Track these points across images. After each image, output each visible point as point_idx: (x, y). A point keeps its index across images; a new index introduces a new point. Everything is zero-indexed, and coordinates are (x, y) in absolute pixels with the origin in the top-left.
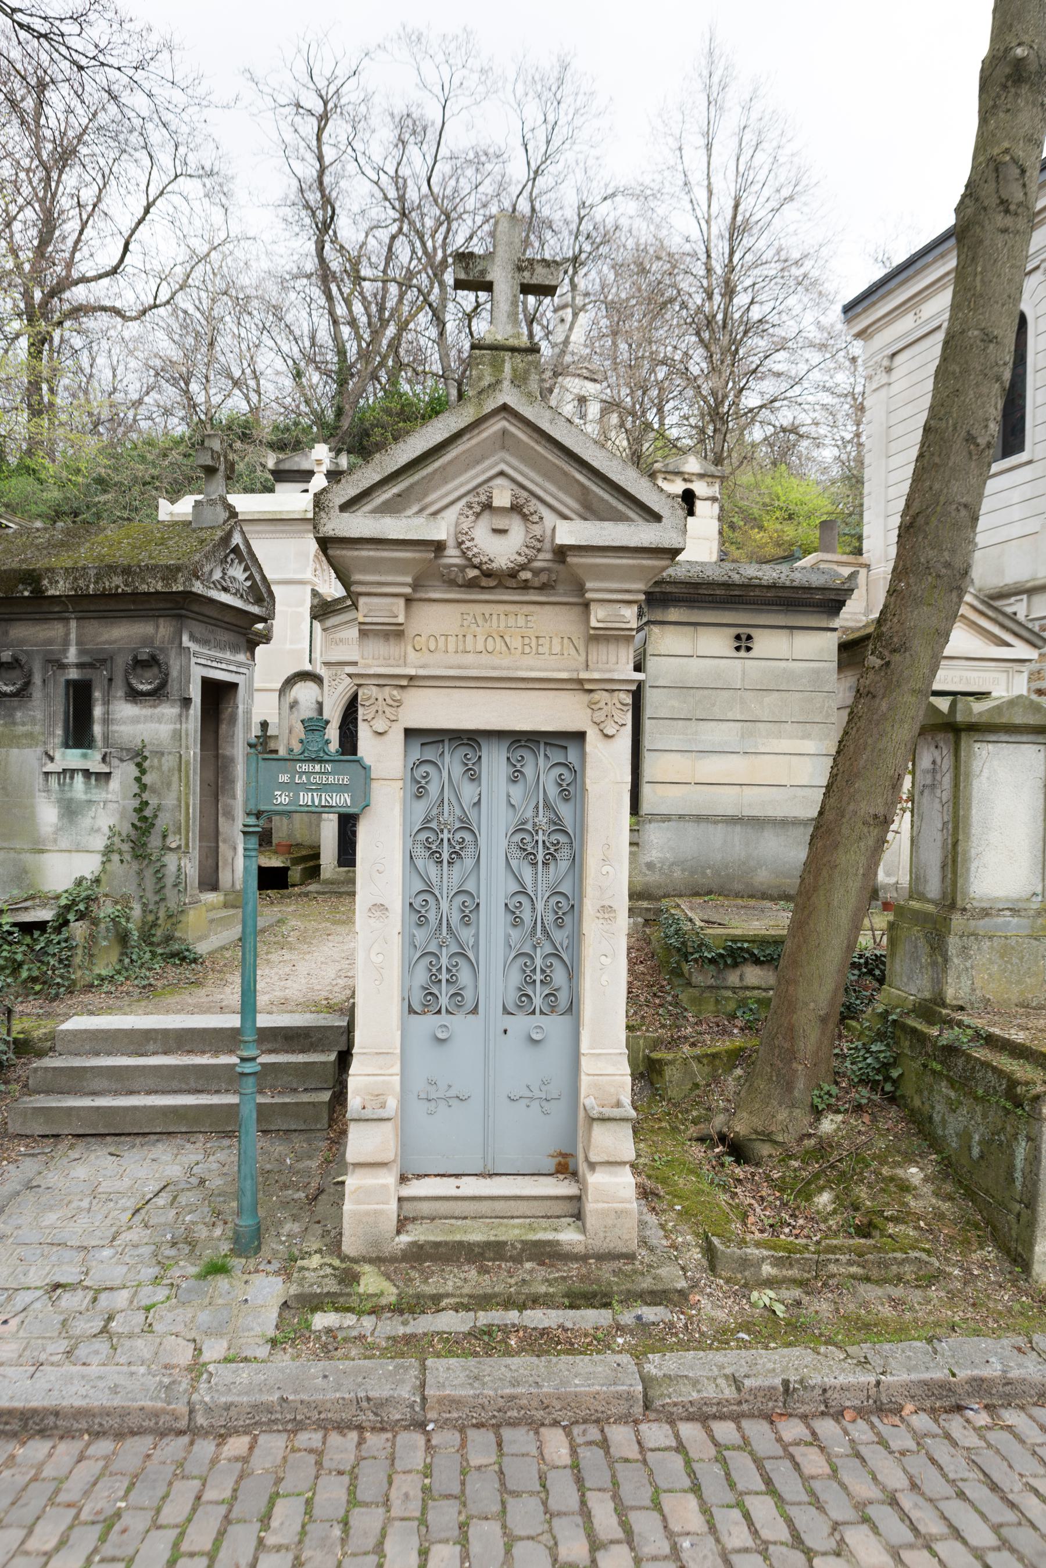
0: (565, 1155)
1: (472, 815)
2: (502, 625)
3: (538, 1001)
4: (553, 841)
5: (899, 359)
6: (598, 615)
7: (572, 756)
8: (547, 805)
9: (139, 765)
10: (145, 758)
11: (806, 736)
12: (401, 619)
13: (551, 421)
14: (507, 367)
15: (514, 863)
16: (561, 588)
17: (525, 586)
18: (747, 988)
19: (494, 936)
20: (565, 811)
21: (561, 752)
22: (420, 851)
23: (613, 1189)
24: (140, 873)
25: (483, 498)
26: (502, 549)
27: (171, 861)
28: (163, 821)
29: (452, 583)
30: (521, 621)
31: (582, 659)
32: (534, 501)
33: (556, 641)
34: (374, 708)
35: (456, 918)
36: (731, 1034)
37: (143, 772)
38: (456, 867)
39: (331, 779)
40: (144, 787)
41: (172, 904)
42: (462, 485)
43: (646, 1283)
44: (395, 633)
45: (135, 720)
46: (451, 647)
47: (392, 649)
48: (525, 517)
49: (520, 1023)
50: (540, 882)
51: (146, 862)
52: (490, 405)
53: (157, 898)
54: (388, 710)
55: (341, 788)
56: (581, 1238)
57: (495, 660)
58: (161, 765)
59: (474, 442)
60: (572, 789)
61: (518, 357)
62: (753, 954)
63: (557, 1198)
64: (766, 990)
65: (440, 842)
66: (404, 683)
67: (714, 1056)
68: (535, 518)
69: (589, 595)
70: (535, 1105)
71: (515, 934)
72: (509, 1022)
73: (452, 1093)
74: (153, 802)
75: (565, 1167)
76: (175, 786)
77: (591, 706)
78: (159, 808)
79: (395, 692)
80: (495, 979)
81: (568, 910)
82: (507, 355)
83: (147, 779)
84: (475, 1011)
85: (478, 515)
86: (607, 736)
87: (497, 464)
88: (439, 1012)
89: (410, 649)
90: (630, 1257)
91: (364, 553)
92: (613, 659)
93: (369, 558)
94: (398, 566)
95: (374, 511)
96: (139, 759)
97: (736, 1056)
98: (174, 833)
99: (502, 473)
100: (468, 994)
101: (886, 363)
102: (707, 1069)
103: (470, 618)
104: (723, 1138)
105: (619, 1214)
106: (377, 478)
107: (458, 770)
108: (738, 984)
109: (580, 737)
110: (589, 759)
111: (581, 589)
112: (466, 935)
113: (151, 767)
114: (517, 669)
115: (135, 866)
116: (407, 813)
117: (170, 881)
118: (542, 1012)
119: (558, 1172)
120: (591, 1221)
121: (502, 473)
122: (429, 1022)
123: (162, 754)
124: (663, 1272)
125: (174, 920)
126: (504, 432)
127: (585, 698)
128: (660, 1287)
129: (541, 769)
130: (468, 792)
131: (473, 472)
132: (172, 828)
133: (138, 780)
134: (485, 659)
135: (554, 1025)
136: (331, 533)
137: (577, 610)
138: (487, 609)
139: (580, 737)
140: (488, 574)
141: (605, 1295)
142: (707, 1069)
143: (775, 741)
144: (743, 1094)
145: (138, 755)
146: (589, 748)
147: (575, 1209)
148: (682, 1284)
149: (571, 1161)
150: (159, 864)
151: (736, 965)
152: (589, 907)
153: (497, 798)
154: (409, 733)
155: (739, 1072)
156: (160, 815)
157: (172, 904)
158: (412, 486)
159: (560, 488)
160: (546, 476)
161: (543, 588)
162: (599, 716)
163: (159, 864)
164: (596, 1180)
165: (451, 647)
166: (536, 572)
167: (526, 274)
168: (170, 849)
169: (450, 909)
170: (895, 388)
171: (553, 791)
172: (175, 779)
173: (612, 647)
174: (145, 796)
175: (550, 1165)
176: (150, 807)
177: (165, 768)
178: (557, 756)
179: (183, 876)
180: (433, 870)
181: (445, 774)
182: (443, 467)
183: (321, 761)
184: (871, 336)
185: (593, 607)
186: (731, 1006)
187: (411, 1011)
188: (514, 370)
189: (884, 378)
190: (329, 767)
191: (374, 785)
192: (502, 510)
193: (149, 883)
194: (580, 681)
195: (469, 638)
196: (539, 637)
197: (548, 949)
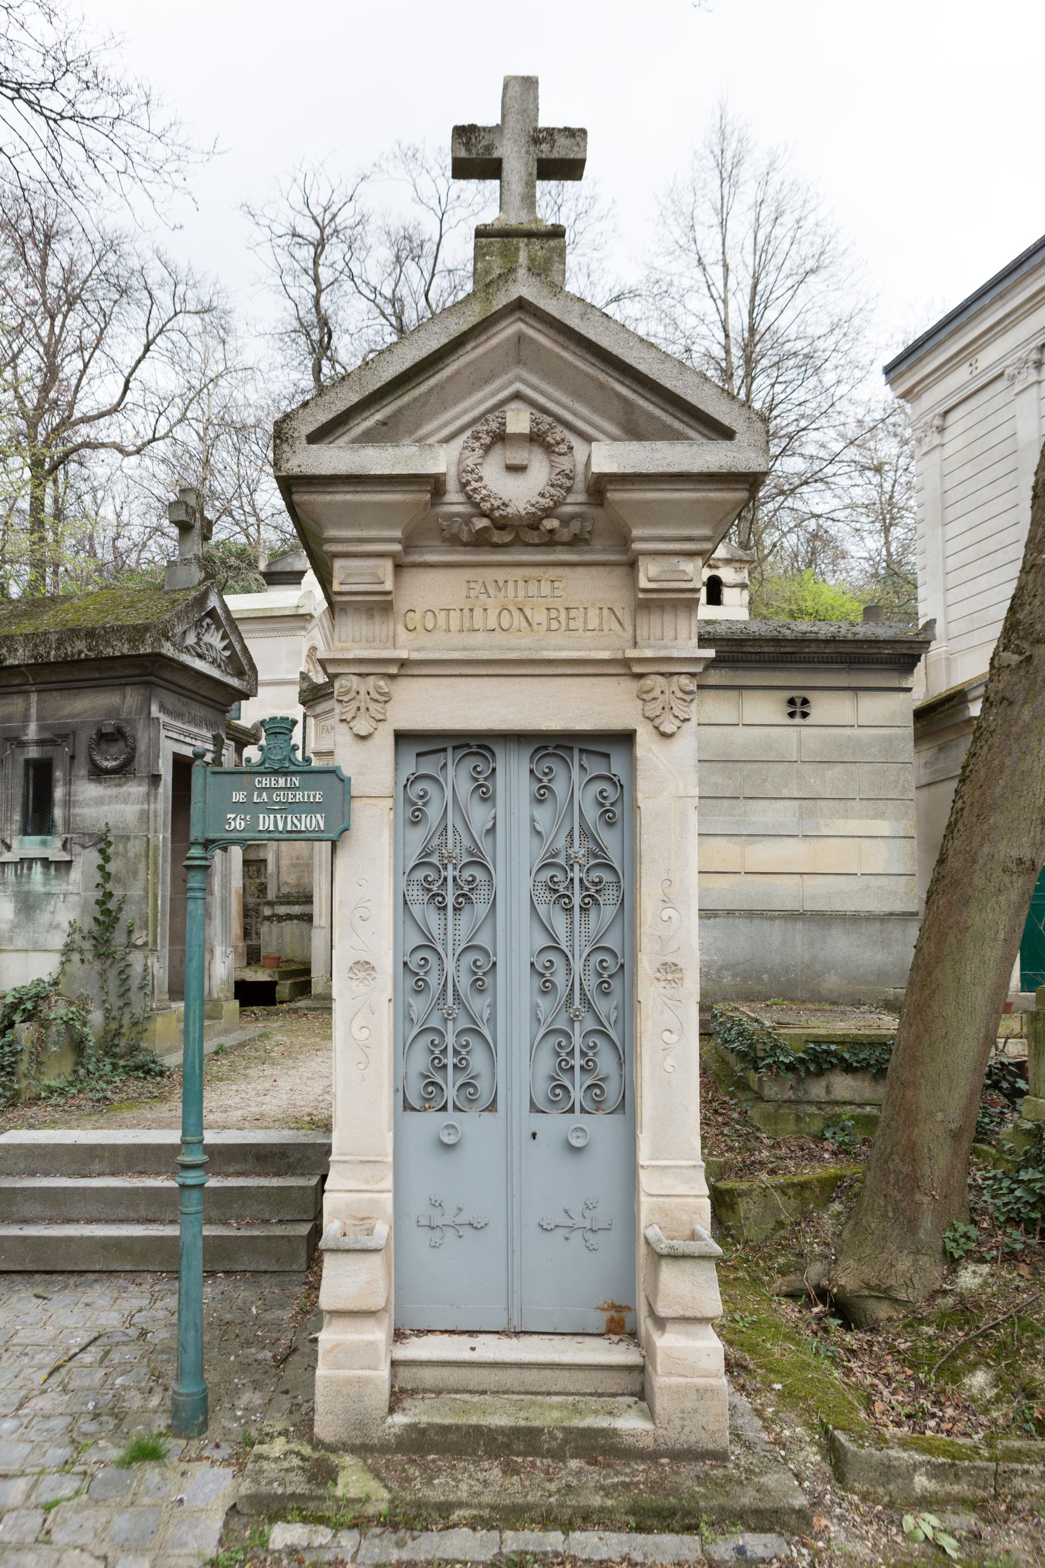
0: (619, 1308)
1: (485, 846)
2: (521, 594)
3: (577, 1095)
4: (596, 879)
5: (953, 417)
6: (649, 573)
7: (617, 766)
8: (586, 833)
9: (102, 851)
10: (110, 843)
11: (880, 815)
12: (388, 586)
13: (582, 316)
14: (523, 258)
15: (541, 909)
16: (597, 543)
17: (551, 541)
18: (836, 1103)
19: (516, 1005)
20: (609, 839)
21: (603, 761)
22: (416, 894)
23: (691, 1357)
25: (494, 426)
26: (520, 491)
27: (137, 959)
28: (127, 916)
29: (454, 541)
30: (546, 588)
31: (628, 634)
32: (559, 428)
33: (593, 613)
34: (354, 705)
35: (465, 983)
36: (821, 1159)
37: (107, 859)
38: (465, 915)
39: (299, 796)
40: (107, 876)
42: (465, 412)
43: (747, 1498)
44: (380, 606)
46: (454, 625)
47: (379, 628)
48: (549, 449)
49: (555, 1125)
50: (577, 934)
51: (109, 961)
52: (501, 300)
54: (373, 706)
55: (312, 808)
56: (648, 1426)
57: (513, 640)
58: (126, 851)
59: (480, 350)
60: (618, 808)
61: (537, 244)
62: (842, 1060)
63: (610, 1368)
64: (861, 1105)
65: (443, 881)
66: (393, 670)
67: (803, 1186)
68: (562, 448)
69: (637, 546)
70: (577, 1237)
71: (545, 1004)
72: (538, 1122)
73: (463, 1218)
74: (118, 893)
75: (620, 1325)
76: (141, 875)
77: (643, 697)
78: (124, 900)
79: (382, 683)
80: (519, 1065)
81: (616, 971)
82: (522, 242)
83: (111, 867)
84: (492, 1107)
85: (487, 449)
86: (664, 735)
87: (511, 383)
88: (444, 1108)
89: (400, 628)
90: (720, 1457)
91: (339, 497)
92: (669, 633)
93: (346, 503)
94: (383, 515)
95: (355, 441)
96: (102, 845)
97: (832, 1187)
98: (141, 928)
99: (517, 396)
100: (483, 1085)
101: (937, 422)
102: (794, 1203)
103: (478, 587)
104: (822, 1294)
105: (702, 1393)
106: (355, 398)
107: (465, 787)
108: (823, 1097)
109: (626, 738)
110: (640, 767)
111: (624, 541)
112: (479, 1004)
113: (116, 853)
114: (543, 649)
115: (97, 966)
116: (398, 843)
117: (135, 983)
118: (583, 1110)
119: (610, 1331)
120: (662, 1403)
121: (517, 396)
122: (431, 1122)
123: (128, 838)
124: (770, 1480)
126: (520, 338)
127: (632, 686)
128: (768, 1504)
129: (576, 784)
130: (479, 815)
131: (480, 395)
132: (138, 923)
133: (101, 868)
134: (498, 638)
135: (600, 1129)
137: (620, 572)
138: (500, 574)
139: (626, 738)
140: (502, 525)
141: (688, 1513)
142: (794, 1203)
143: (841, 822)
144: (846, 1235)
145: (101, 840)
146: (640, 751)
147: (638, 1385)
148: (800, 1501)
149: (627, 1316)
150: (123, 964)
151: (820, 1073)
152: (646, 965)
153: (518, 821)
154: (402, 737)
155: (837, 1207)
156: (125, 907)
158: (400, 411)
159: (595, 409)
160: (577, 394)
161: (576, 542)
162: (654, 709)
163: (123, 964)
164: (668, 1343)
165: (454, 625)
166: (565, 521)
167: (545, 147)
168: (136, 947)
169: (457, 971)
170: (949, 449)
171: (592, 814)
172: (142, 866)
173: (668, 618)
174: (109, 887)
175: (599, 1320)
176: (115, 899)
177: (131, 854)
178: (596, 767)
179: (149, 978)
180: (434, 919)
181: (448, 792)
182: (441, 386)
183: (286, 774)
184: (918, 396)
185: (642, 562)
186: (817, 1126)
187: (407, 1107)
188: (532, 259)
189: (936, 440)
190: (296, 780)
191: (356, 805)
192: (518, 437)
193: (113, 986)
194: (626, 662)
195: (478, 612)
196: (572, 608)
197: (590, 1024)
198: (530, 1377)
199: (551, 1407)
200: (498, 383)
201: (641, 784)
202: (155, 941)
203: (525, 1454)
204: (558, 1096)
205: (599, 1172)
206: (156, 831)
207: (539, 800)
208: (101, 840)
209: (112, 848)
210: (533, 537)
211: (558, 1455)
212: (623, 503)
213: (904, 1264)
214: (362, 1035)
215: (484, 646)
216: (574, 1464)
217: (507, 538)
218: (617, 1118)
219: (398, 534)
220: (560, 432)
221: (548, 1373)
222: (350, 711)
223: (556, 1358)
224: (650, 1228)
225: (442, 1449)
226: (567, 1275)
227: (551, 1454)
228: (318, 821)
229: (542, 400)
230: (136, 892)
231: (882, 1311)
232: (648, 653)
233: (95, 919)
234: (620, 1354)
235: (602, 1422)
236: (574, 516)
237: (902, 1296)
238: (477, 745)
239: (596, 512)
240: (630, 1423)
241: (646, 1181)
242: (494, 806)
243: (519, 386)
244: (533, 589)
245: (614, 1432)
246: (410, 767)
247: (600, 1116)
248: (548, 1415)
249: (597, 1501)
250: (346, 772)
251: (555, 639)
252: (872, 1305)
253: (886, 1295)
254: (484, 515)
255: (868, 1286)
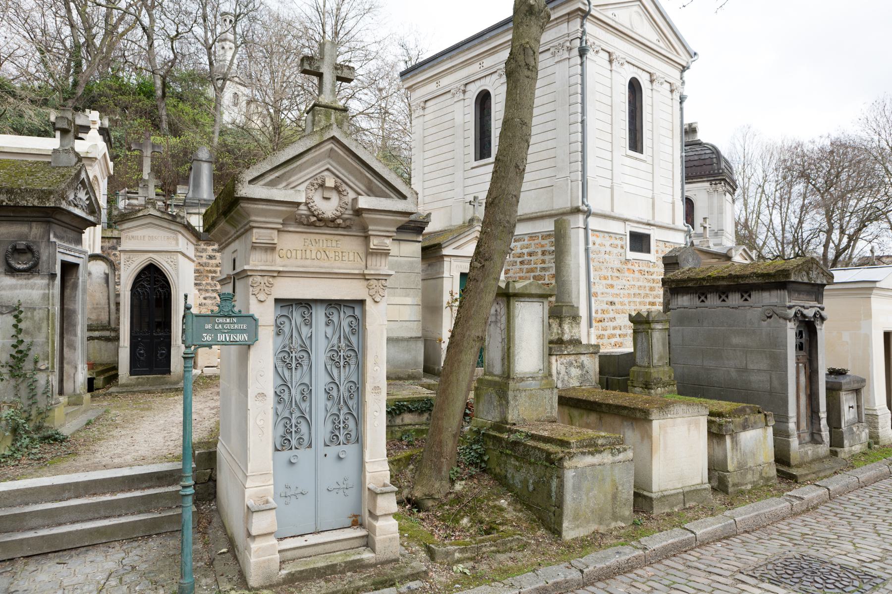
0: (355, 516)
1: (307, 343)
2: (325, 245)
3: (342, 438)
4: (350, 354)
6: (374, 243)
7: (357, 312)
8: (346, 338)
9: (16, 317)
10: (21, 312)
11: (407, 295)
12: (275, 242)
15: (329, 367)
16: (354, 228)
17: (338, 226)
19: (320, 403)
20: (354, 339)
21: (351, 310)
22: (280, 364)
23: (387, 528)
24: (16, 387)
25: (320, 181)
26: (329, 207)
27: (41, 378)
28: (34, 353)
29: (300, 223)
30: (334, 244)
31: (364, 263)
32: (344, 185)
33: (351, 254)
34: (258, 288)
35: (298, 397)
37: (19, 321)
38: (299, 371)
40: (20, 331)
41: (42, 405)
42: (308, 174)
44: (271, 248)
45: (13, 287)
46: (299, 256)
47: (269, 256)
48: (339, 192)
49: (333, 450)
50: (344, 376)
51: (22, 379)
53: (30, 402)
54: (266, 289)
55: (242, 331)
56: (373, 555)
57: (321, 263)
58: (33, 316)
59: (317, 153)
60: (359, 327)
63: (357, 538)
65: (290, 359)
66: (275, 274)
68: (345, 193)
69: (370, 233)
70: (341, 492)
71: (329, 404)
72: (327, 450)
73: (299, 491)
74: (27, 340)
75: (357, 522)
76: (44, 329)
77: (369, 287)
78: (32, 344)
79: (271, 279)
80: (322, 429)
81: (358, 389)
83: (22, 325)
84: (310, 446)
85: (316, 189)
86: (376, 302)
88: (291, 449)
89: (277, 256)
91: (260, 206)
92: (379, 264)
93: (262, 209)
94: (277, 214)
95: (265, 185)
96: (16, 313)
98: (44, 360)
99: (328, 169)
100: (306, 437)
103: (308, 242)
104: (409, 500)
105: (391, 540)
106: (269, 168)
107: (299, 320)
109: (362, 302)
110: (368, 314)
112: (304, 406)
113: (26, 318)
114: (333, 268)
115: (13, 382)
116: (275, 343)
117: (40, 391)
119: (353, 525)
120: (378, 546)
121: (328, 169)
122: (286, 454)
123: (35, 309)
125: (43, 415)
127: (365, 283)
129: (344, 319)
130: (305, 331)
131: (314, 168)
132: (42, 357)
133: (15, 326)
134: (316, 262)
135: (350, 450)
136: (244, 195)
137: (361, 239)
138: (317, 237)
139: (362, 302)
140: (320, 220)
143: (392, 298)
145: (15, 309)
146: (367, 308)
147: (368, 542)
149: (359, 519)
150: (31, 380)
152: (369, 387)
153: (321, 332)
156: (33, 348)
157: (42, 405)
158: (285, 173)
161: (347, 227)
162: (372, 292)
163: (31, 380)
164: (380, 524)
165: (299, 256)
166: (345, 220)
168: (40, 370)
169: (296, 393)
171: (347, 329)
172: (44, 325)
173: (379, 258)
174: (21, 337)
175: (349, 522)
176: (25, 344)
177: (37, 318)
178: (349, 312)
179: (50, 387)
180: (287, 373)
181: (293, 322)
182: (301, 165)
183: (230, 317)
185: (372, 238)
187: (276, 450)
192: (330, 188)
193: (24, 392)
194: (364, 275)
195: (308, 252)
196: (344, 252)
198: (328, 548)
199: (338, 556)
200: (321, 163)
201: (368, 320)
202: (53, 367)
203: (330, 575)
204: (334, 438)
205: (349, 467)
206: (53, 305)
207: (327, 325)
208: (15, 309)
209: (23, 314)
210: (332, 225)
211: (343, 572)
212: (367, 218)
213: (437, 485)
214: (260, 423)
215: (312, 265)
216: (349, 574)
217: (322, 224)
218: (356, 445)
219: (281, 221)
220: (344, 187)
221: (334, 544)
222: (256, 291)
223: (338, 538)
224: (370, 483)
225: (300, 580)
226: (338, 507)
227: (340, 572)
228: (245, 337)
229: (337, 173)
230: (40, 339)
231: (430, 503)
232: (372, 272)
233: (11, 355)
234: (362, 533)
235: (357, 557)
236: (347, 219)
237: (437, 497)
238: (306, 304)
239: (357, 218)
240: (367, 556)
241: (368, 467)
242: (311, 327)
243: (328, 166)
244: (329, 244)
245: (362, 560)
246: (279, 313)
247: (349, 445)
248: (338, 559)
249: (361, 583)
250: (256, 316)
251: (338, 264)
252: (426, 501)
253: (431, 497)
254: (314, 216)
255: (425, 495)
